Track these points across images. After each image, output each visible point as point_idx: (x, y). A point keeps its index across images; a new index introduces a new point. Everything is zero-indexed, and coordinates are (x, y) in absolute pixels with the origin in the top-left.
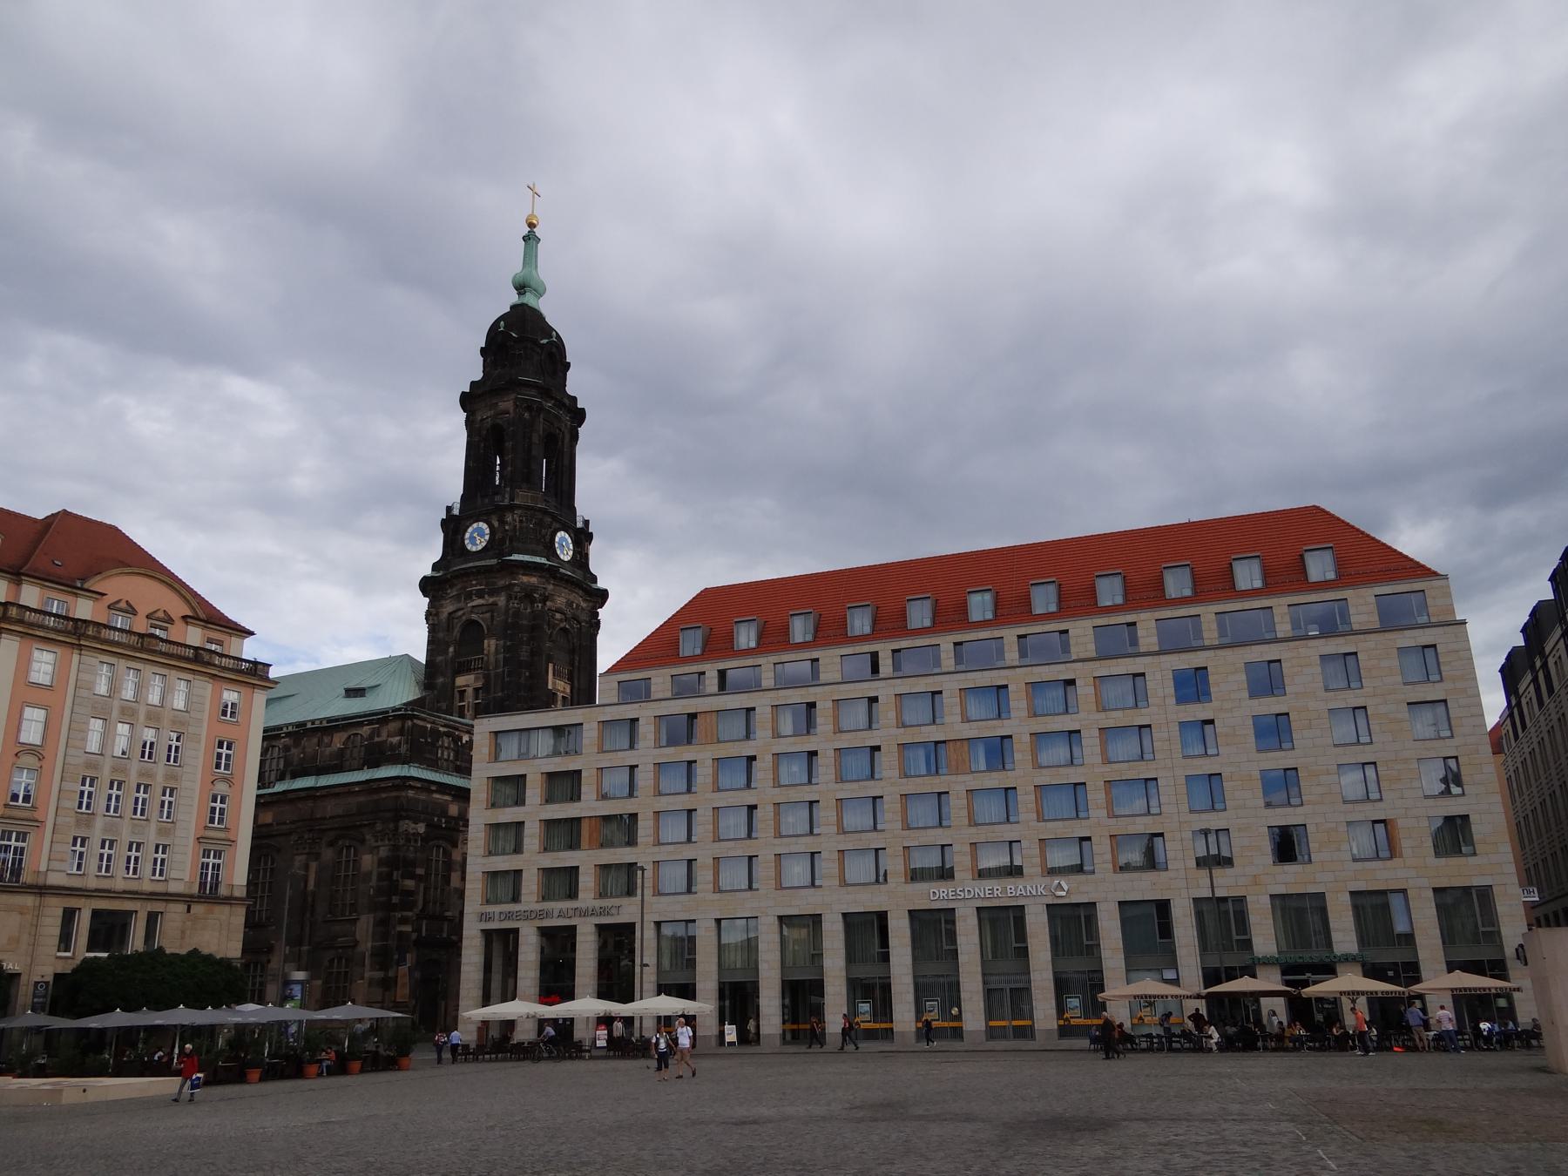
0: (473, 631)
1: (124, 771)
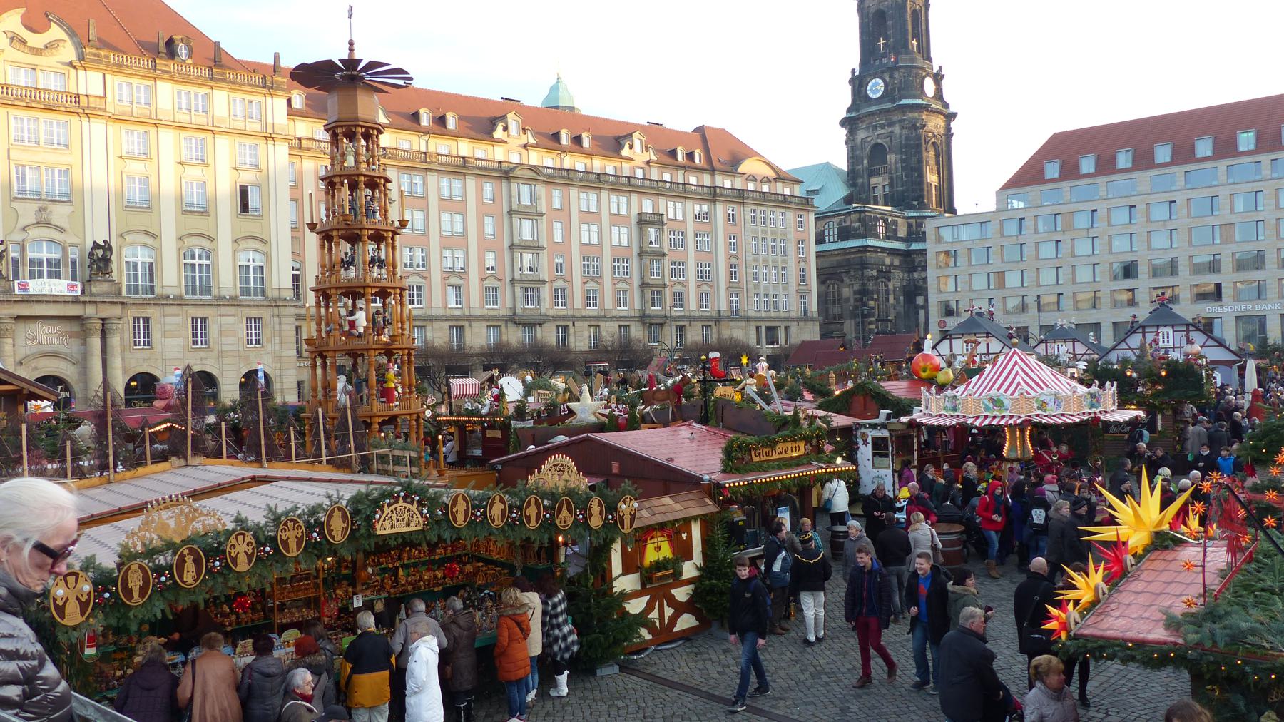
0: (878, 152)
1: (767, 261)
